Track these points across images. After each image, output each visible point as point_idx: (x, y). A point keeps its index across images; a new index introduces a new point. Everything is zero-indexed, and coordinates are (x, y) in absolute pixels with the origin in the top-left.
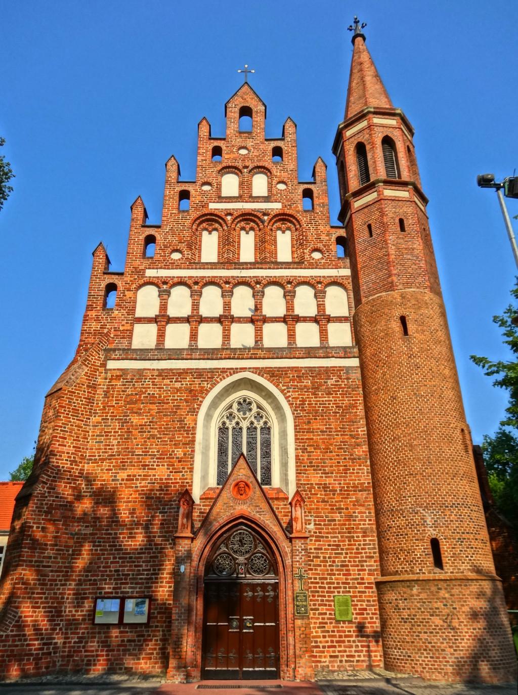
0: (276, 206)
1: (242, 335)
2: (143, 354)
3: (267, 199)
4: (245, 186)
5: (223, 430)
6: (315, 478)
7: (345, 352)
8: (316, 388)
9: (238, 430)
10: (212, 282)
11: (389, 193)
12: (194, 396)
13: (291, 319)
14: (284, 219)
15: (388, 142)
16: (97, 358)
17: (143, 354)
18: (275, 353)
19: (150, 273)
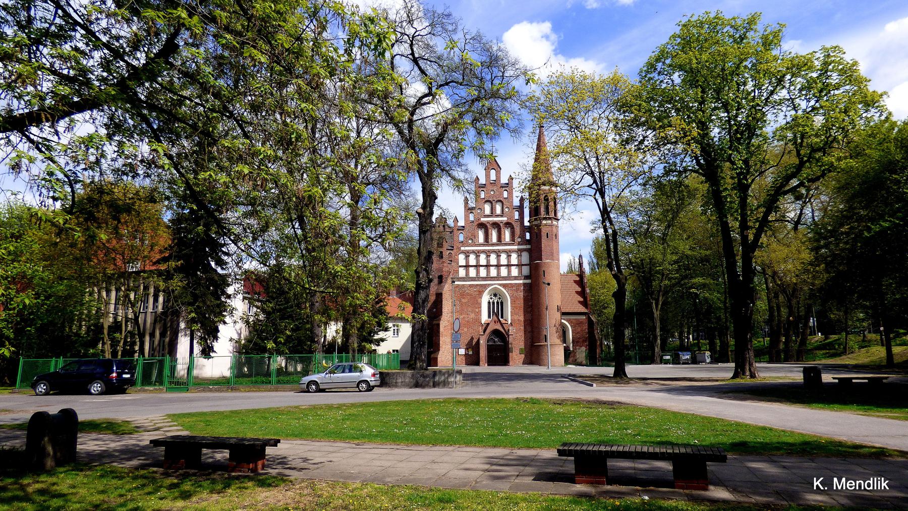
0: (505, 219)
1: (493, 272)
2: (463, 279)
3: (502, 216)
4: (493, 209)
5: (489, 303)
6: (516, 317)
7: (526, 277)
8: (517, 290)
9: (493, 303)
10: (483, 252)
11: (544, 222)
12: (481, 293)
13: (509, 266)
14: (508, 225)
15: (546, 199)
16: (449, 281)
17: (463, 279)
18: (504, 278)
19: (462, 248)
